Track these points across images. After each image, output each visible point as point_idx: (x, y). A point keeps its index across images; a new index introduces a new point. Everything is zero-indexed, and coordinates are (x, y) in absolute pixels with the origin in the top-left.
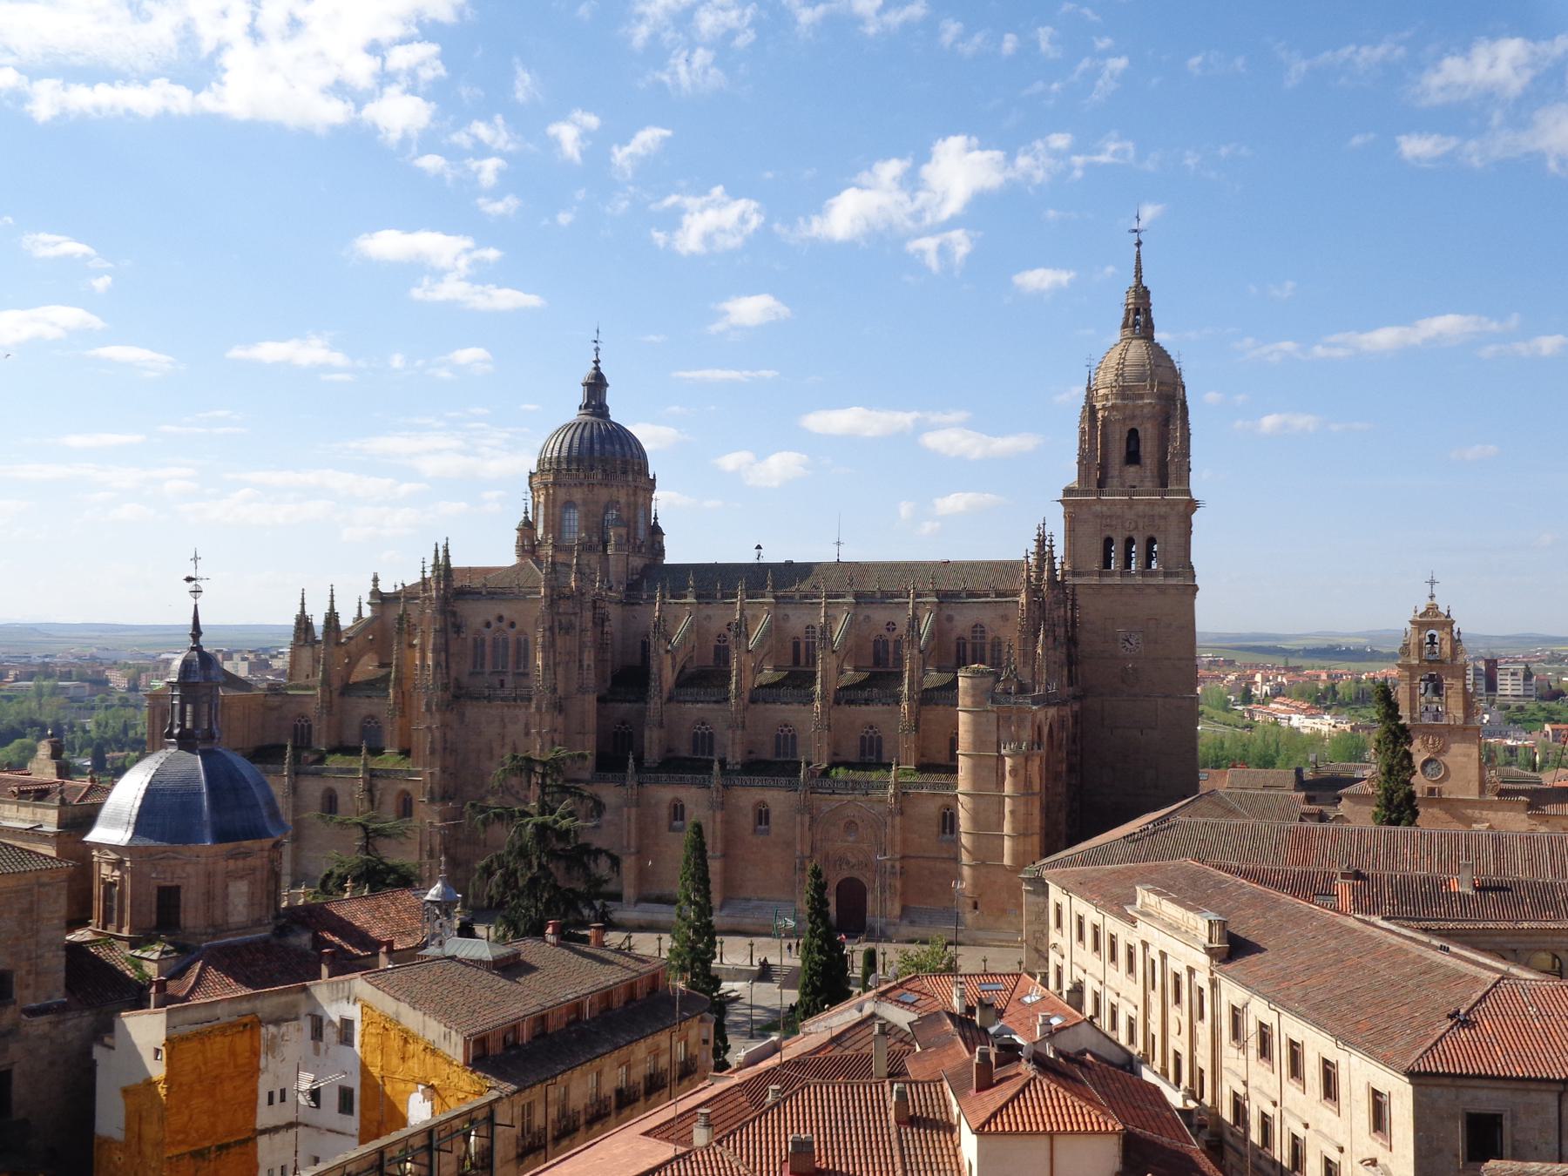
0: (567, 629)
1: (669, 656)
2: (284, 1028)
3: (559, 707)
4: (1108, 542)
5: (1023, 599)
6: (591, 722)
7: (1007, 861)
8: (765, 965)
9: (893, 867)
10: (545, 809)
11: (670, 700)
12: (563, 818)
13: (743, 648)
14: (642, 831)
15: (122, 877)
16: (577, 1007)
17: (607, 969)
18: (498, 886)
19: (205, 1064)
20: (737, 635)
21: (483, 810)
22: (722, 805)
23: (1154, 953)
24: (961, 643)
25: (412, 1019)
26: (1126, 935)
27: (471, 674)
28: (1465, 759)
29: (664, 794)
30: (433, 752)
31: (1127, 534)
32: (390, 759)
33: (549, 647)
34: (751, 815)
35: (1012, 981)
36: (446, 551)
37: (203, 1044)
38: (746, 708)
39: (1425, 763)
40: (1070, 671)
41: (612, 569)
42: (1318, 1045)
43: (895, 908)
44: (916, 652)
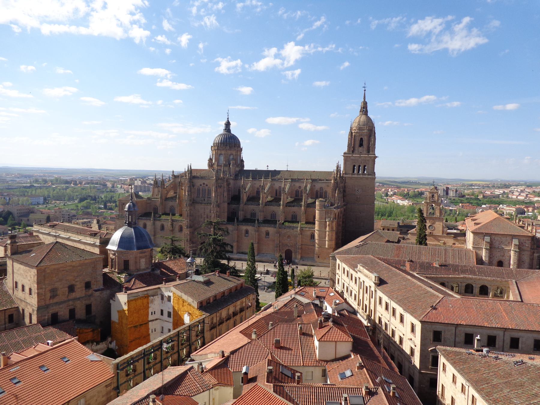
0: (220, 187)
1: (245, 194)
2: (155, 297)
3: (218, 206)
4: (354, 166)
5: (332, 181)
6: (226, 210)
7: (327, 247)
8: (267, 271)
9: (299, 247)
10: (215, 234)
11: (245, 204)
12: (220, 236)
13: (263, 192)
14: (238, 236)
15: (115, 257)
16: (224, 293)
17: (230, 283)
18: (204, 252)
19: (136, 306)
20: (262, 189)
21: (200, 234)
22: (258, 231)
23: (361, 280)
24: (317, 192)
25: (185, 297)
26: (355, 275)
27: (197, 197)
28: (439, 226)
29: (244, 228)
30: (187, 216)
31: (359, 164)
32: (177, 217)
33: (216, 191)
34: (265, 234)
35: (327, 289)
36: (191, 167)
37: (136, 301)
38: (264, 207)
39: (430, 226)
40: (343, 199)
41: (231, 171)
42: (399, 310)
43: (299, 257)
44: (306, 195)
